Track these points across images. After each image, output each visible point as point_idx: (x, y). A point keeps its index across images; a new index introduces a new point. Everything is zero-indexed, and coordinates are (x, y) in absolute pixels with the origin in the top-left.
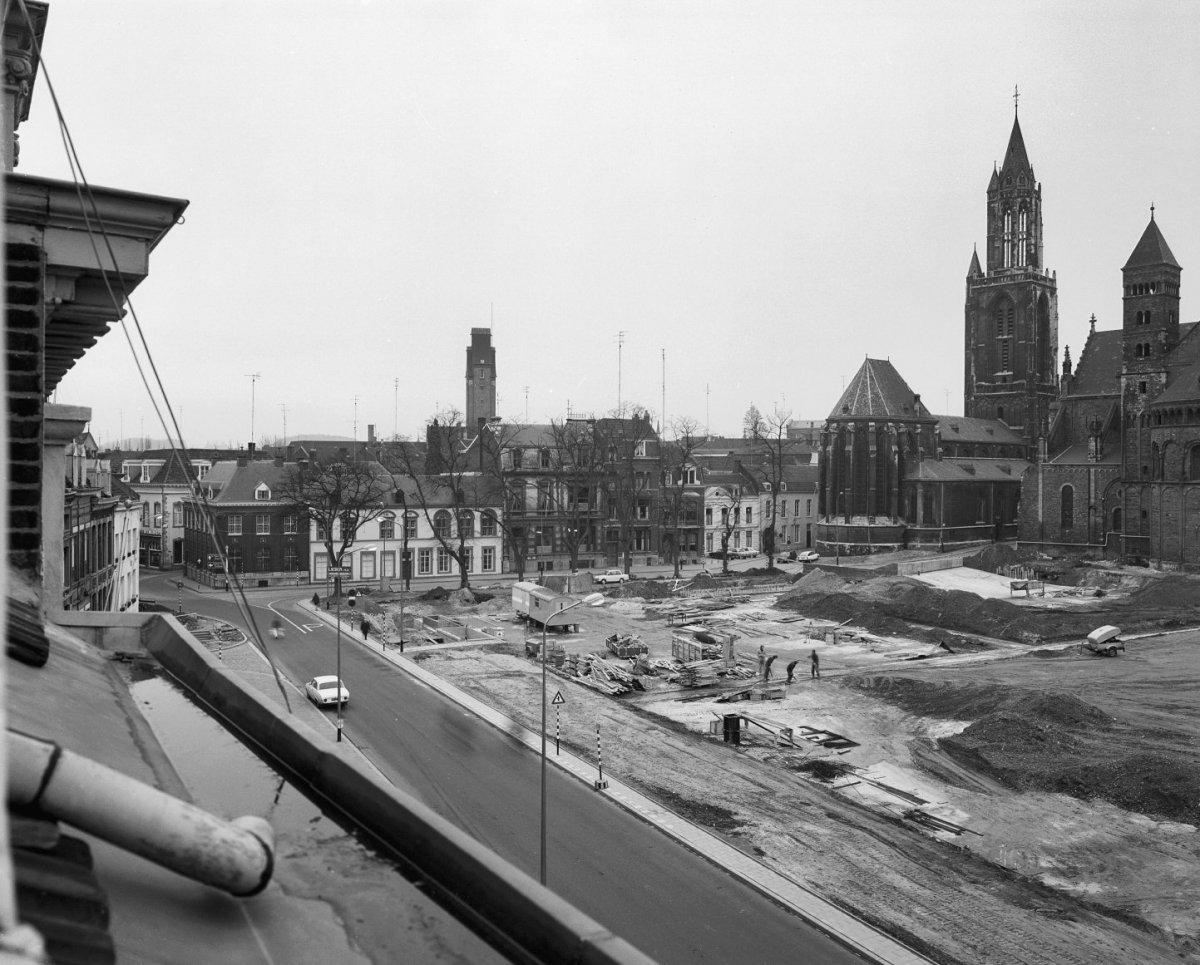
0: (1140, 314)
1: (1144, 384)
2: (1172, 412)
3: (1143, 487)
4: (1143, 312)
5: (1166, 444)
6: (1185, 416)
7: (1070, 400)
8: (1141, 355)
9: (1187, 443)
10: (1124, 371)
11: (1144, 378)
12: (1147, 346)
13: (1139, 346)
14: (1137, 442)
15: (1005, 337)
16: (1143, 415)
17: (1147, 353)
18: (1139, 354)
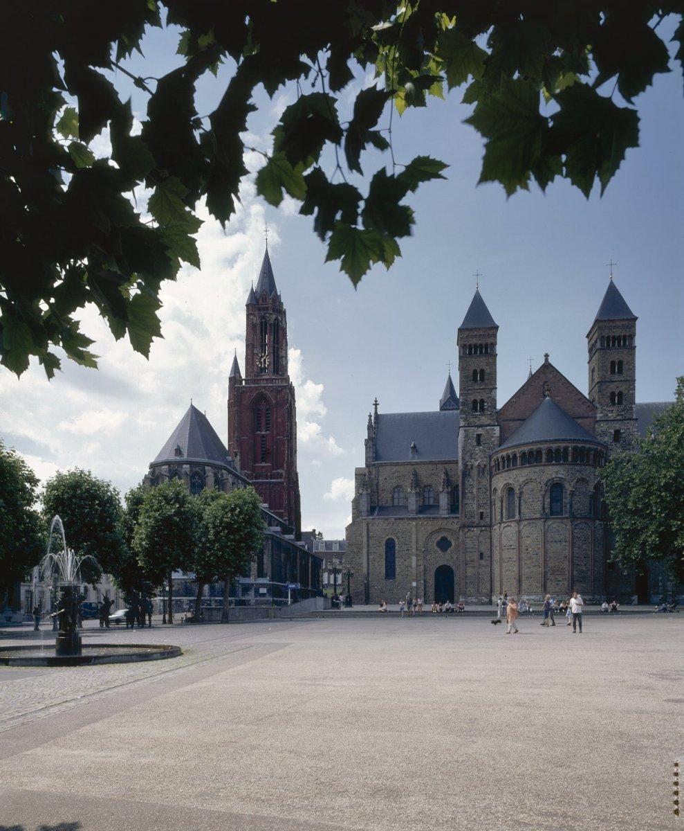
0: (475, 372)
1: (479, 436)
2: (531, 452)
3: (481, 531)
4: (479, 370)
5: (526, 483)
6: (544, 456)
7: (374, 465)
8: (476, 411)
9: (547, 482)
10: (462, 424)
11: (480, 431)
12: (482, 401)
13: (475, 402)
14: (475, 491)
15: (264, 433)
16: (479, 466)
17: (482, 409)
18: (475, 409)
